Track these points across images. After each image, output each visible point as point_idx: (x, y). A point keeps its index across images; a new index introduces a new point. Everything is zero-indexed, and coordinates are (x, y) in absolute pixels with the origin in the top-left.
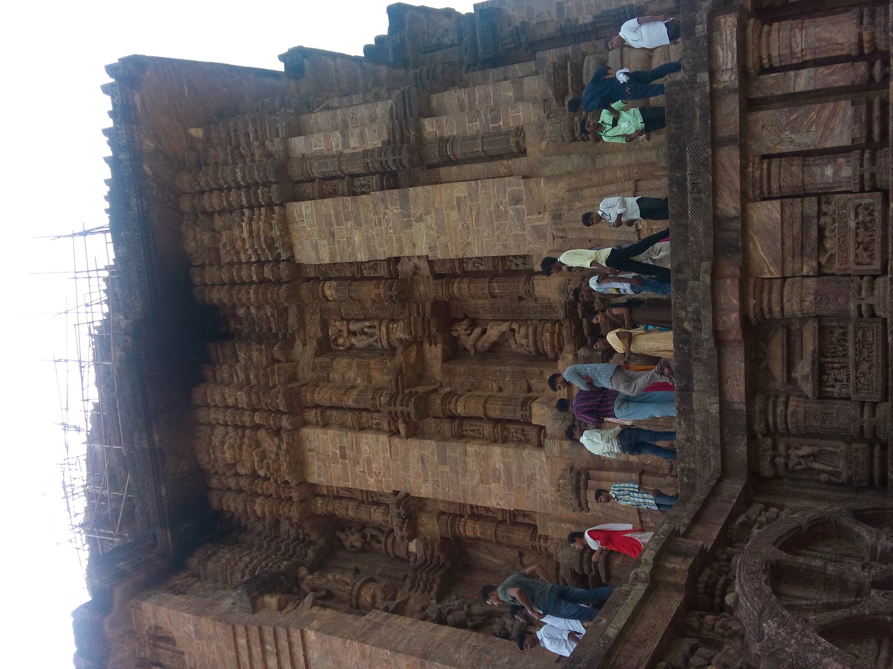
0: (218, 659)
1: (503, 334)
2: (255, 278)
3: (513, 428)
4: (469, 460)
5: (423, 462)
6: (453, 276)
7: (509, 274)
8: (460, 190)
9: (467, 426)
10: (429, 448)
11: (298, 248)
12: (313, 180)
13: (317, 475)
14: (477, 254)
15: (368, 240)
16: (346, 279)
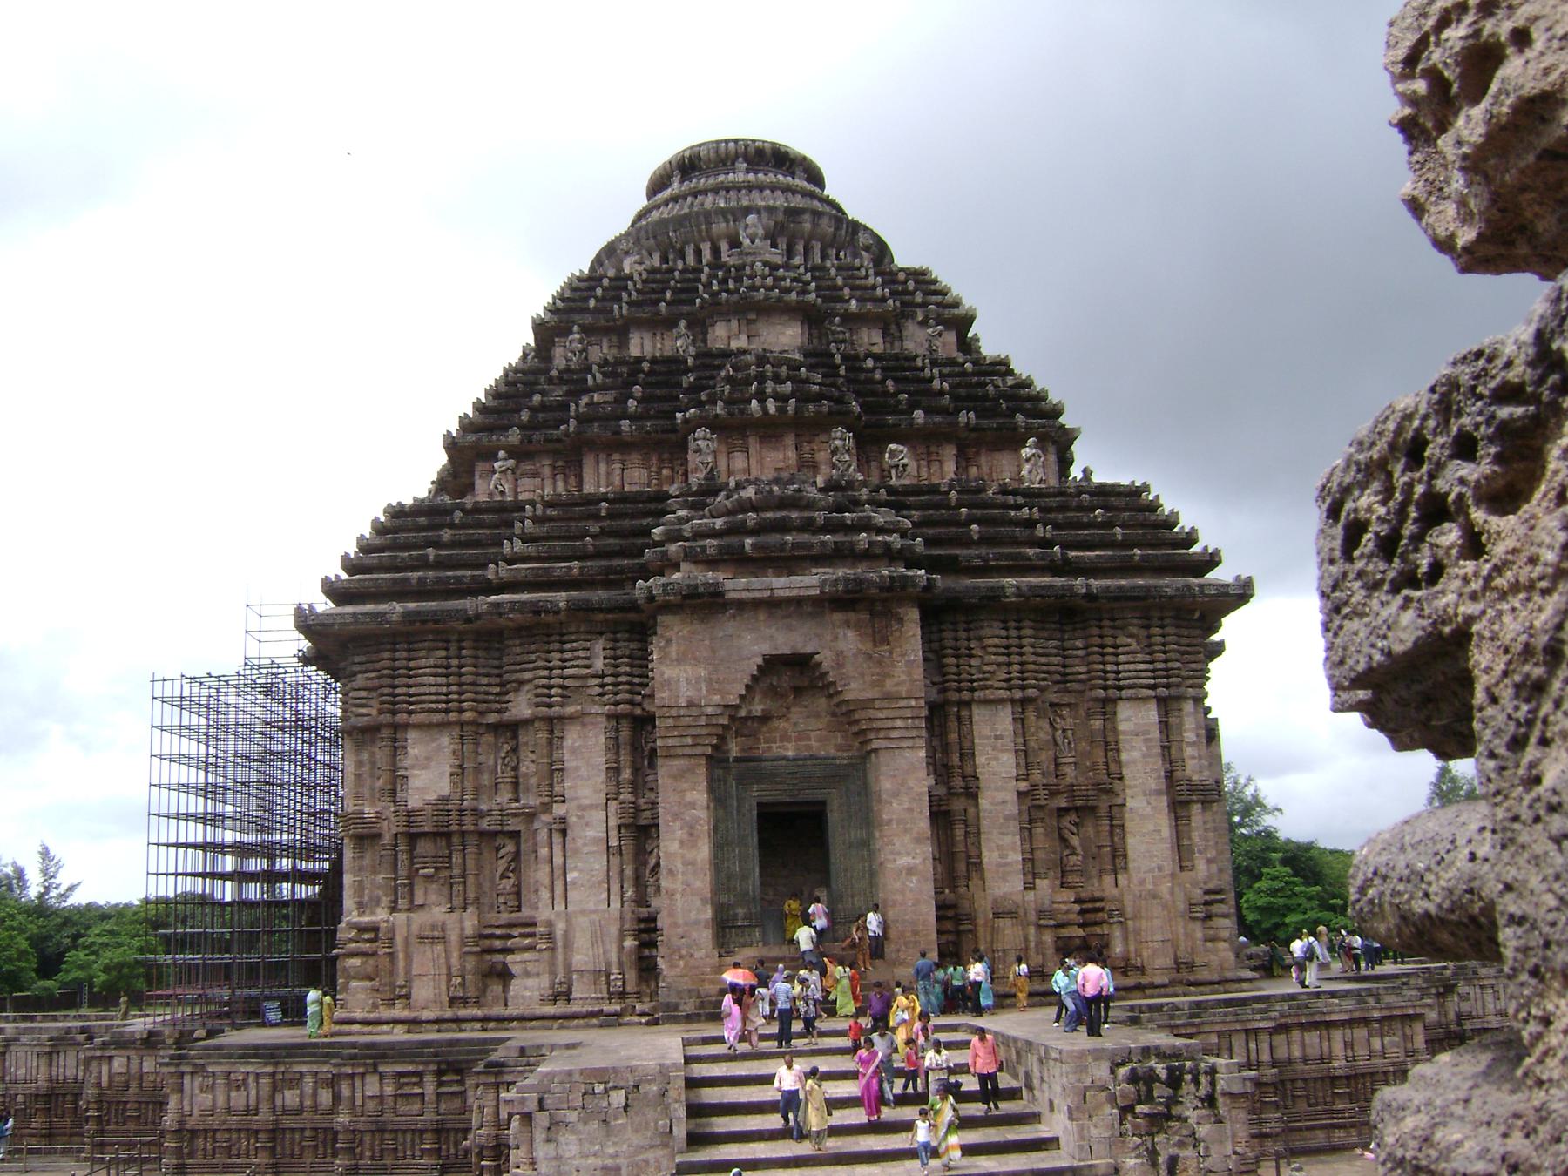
0: (896, 680)
1: (1074, 848)
2: (1109, 667)
3: (1029, 865)
4: (1010, 837)
5: (1004, 802)
6: (1111, 819)
7: (1114, 857)
8: (1166, 831)
9: (1026, 833)
10: (1013, 808)
11: (1128, 704)
12: (1167, 715)
13: (978, 713)
14: (1131, 841)
15: (1134, 762)
16: (1105, 737)
